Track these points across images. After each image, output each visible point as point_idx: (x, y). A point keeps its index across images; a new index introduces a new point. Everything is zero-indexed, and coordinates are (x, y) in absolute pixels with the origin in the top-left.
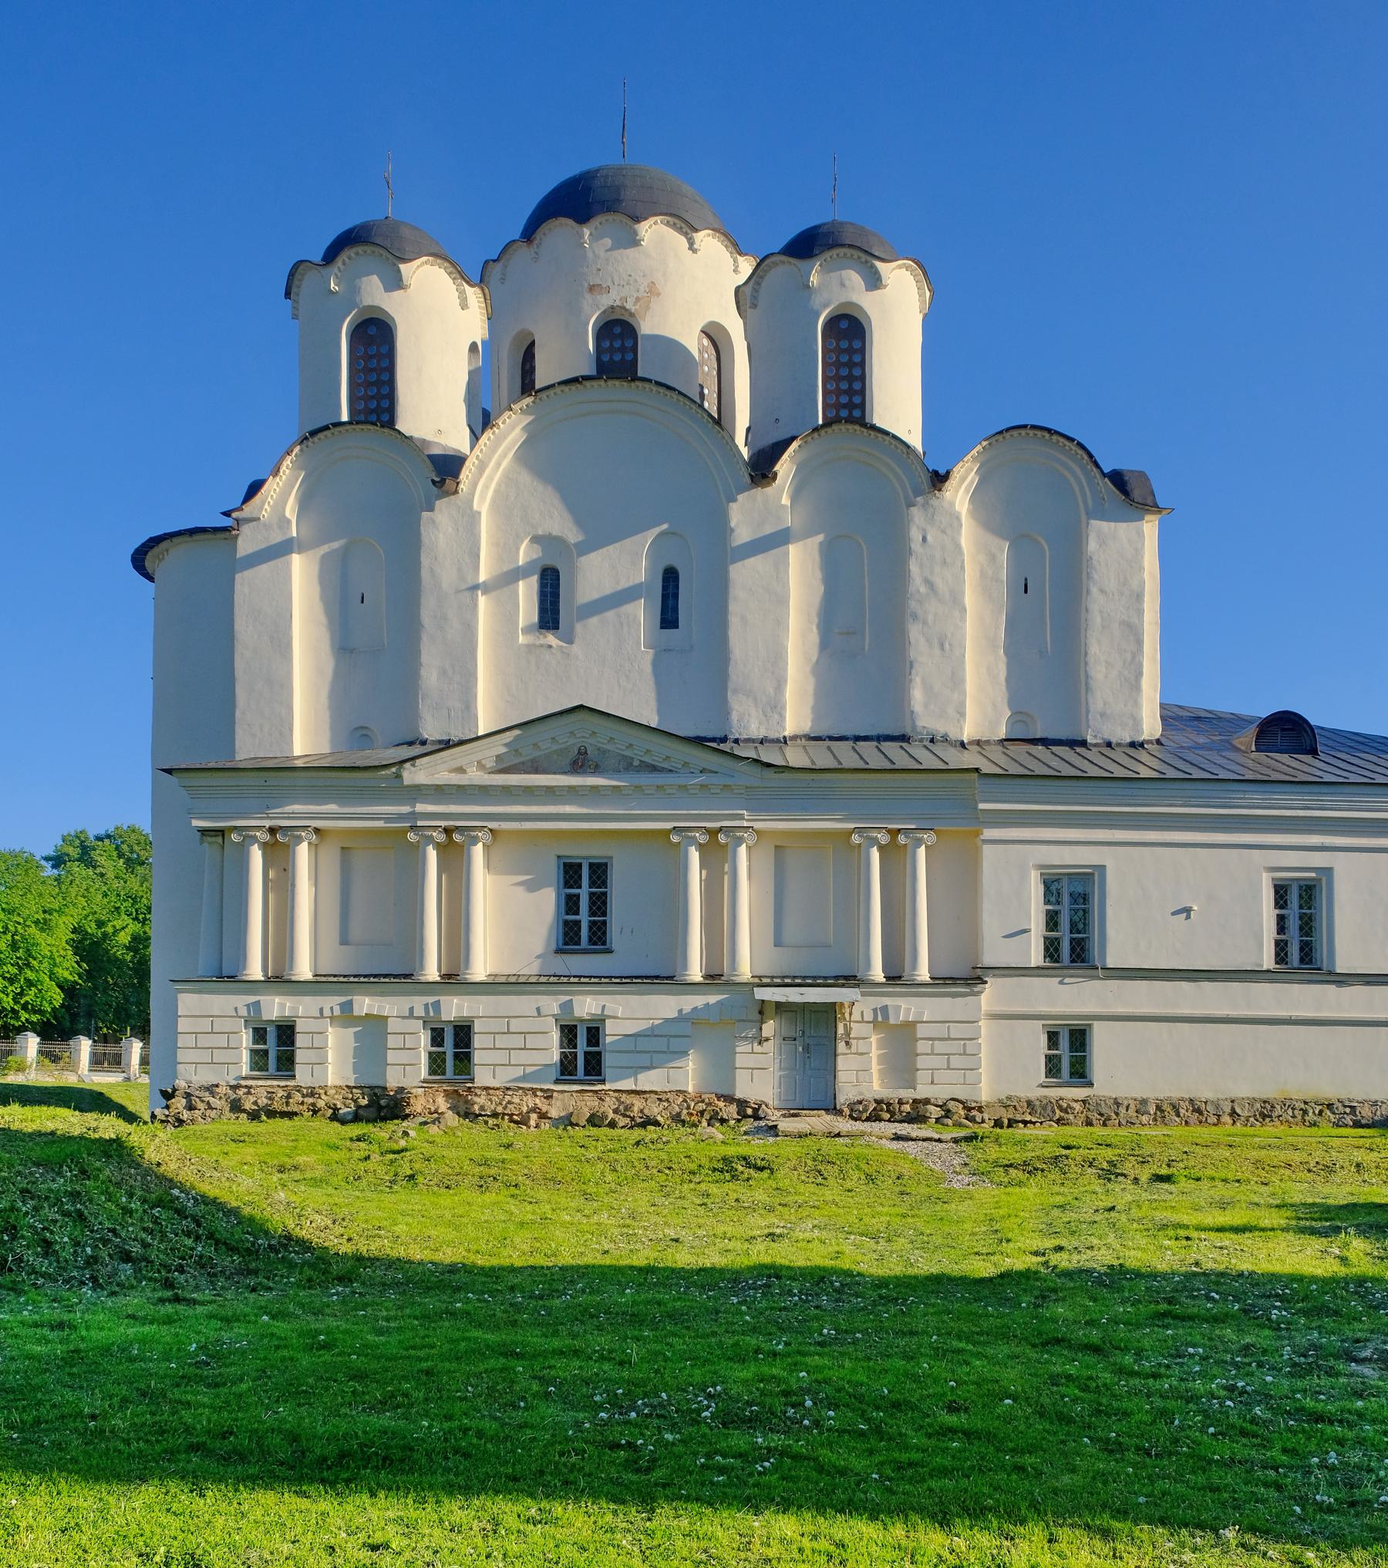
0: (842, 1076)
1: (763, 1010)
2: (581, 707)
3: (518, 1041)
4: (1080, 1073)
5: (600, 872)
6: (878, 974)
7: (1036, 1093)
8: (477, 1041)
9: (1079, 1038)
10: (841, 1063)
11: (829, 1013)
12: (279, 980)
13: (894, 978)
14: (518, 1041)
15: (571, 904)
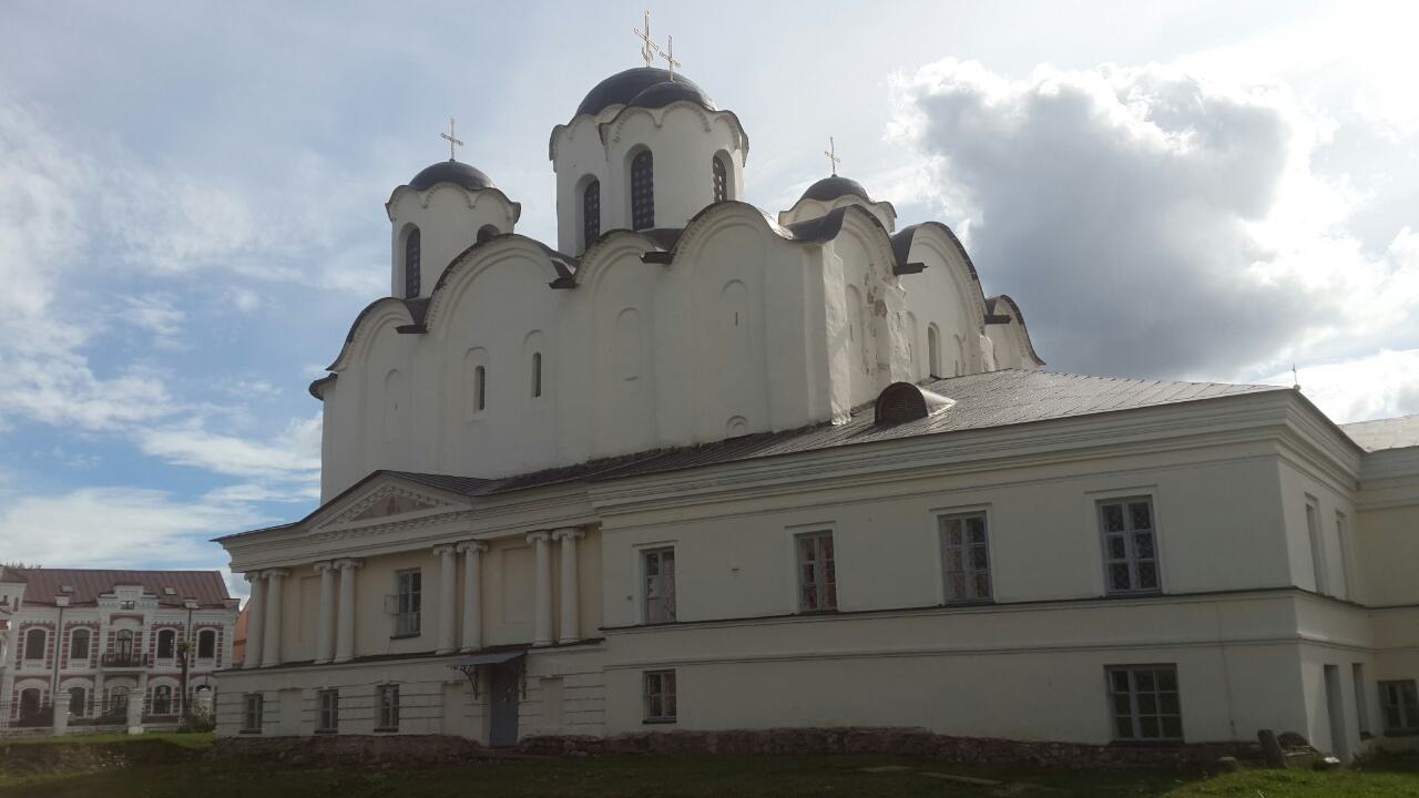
2: (377, 474)
10: (522, 710)
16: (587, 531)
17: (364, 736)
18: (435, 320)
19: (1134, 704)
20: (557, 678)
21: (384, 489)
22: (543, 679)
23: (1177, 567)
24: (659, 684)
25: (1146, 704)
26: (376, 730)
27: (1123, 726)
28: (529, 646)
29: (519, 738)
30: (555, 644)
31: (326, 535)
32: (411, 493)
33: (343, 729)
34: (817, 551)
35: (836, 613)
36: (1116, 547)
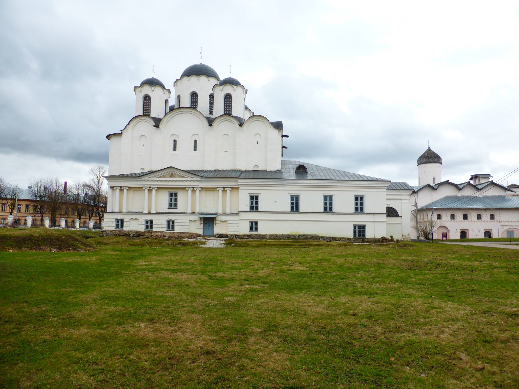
0: (214, 230)
3: (160, 223)
5: (176, 195)
8: (154, 223)
9: (256, 223)
10: (214, 228)
14: (160, 223)
15: (171, 200)
17: (162, 232)
18: (162, 125)
19: (357, 231)
20: (226, 221)
21: (170, 171)
22: (221, 221)
23: (367, 208)
25: (359, 231)
26: (167, 230)
27: (355, 235)
28: (216, 214)
29: (214, 234)
30: (224, 214)
31: (148, 180)
32: (180, 173)
33: (154, 229)
35: (299, 212)
36: (357, 204)
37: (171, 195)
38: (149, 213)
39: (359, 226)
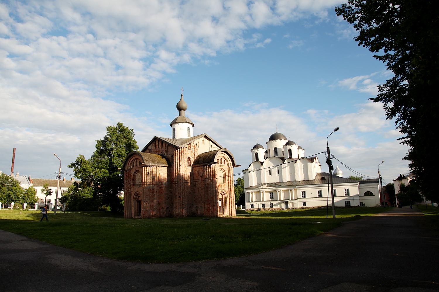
1: (283, 202)
4: (305, 205)
5: (272, 193)
6: (291, 199)
7: (302, 207)
9: (305, 203)
11: (288, 202)
12: (252, 202)
13: (292, 199)
15: (271, 196)
16: (295, 190)
24: (304, 204)
25: (348, 204)
27: (346, 205)
34: (320, 192)
37: (270, 193)
38: (263, 201)
39: (348, 202)
